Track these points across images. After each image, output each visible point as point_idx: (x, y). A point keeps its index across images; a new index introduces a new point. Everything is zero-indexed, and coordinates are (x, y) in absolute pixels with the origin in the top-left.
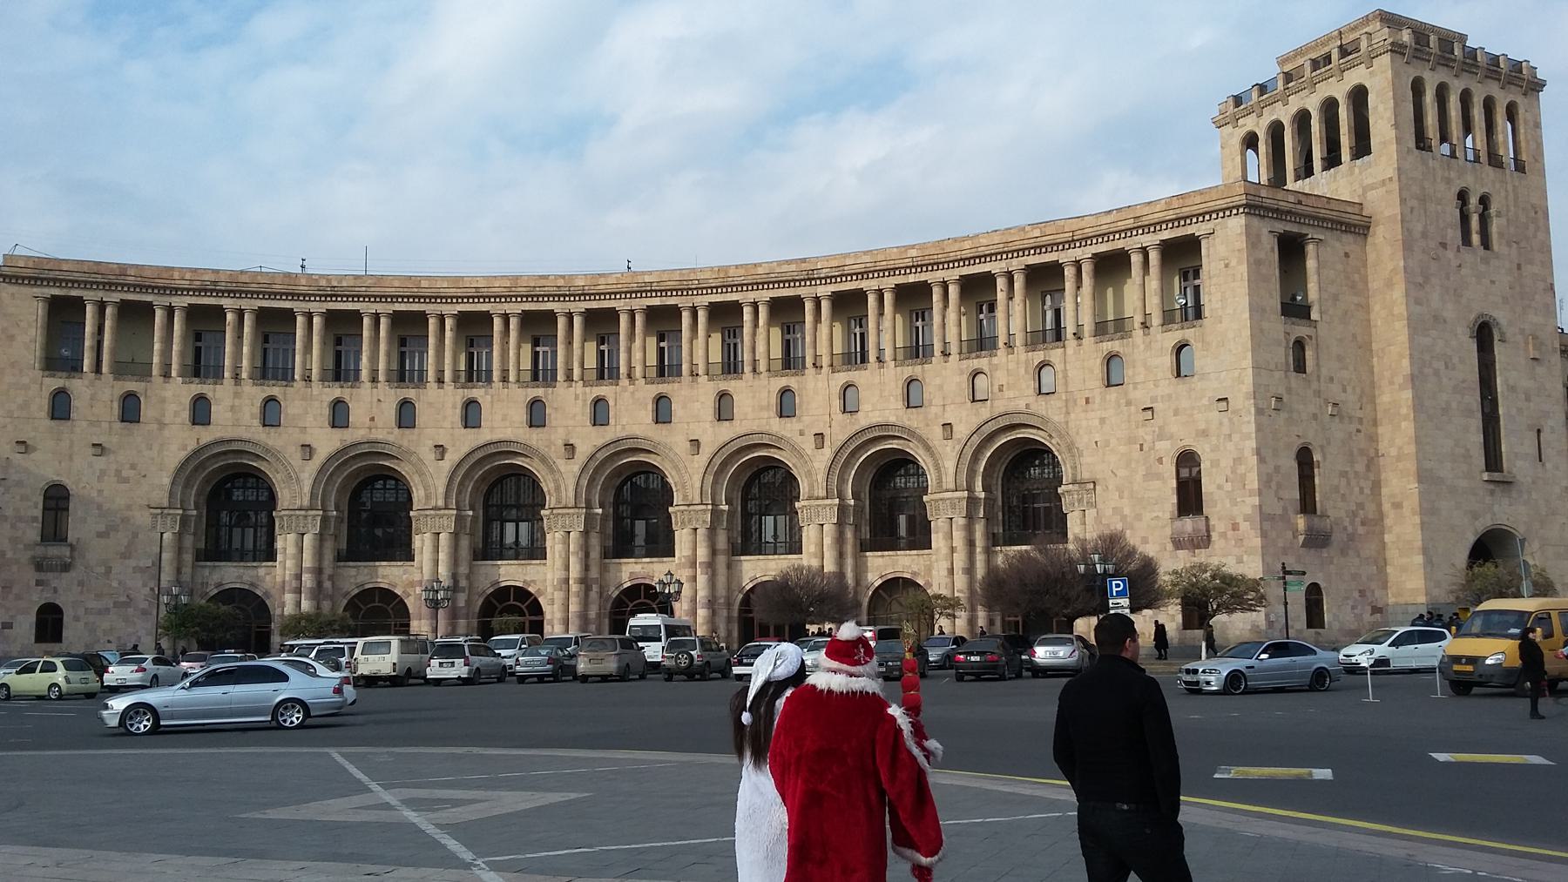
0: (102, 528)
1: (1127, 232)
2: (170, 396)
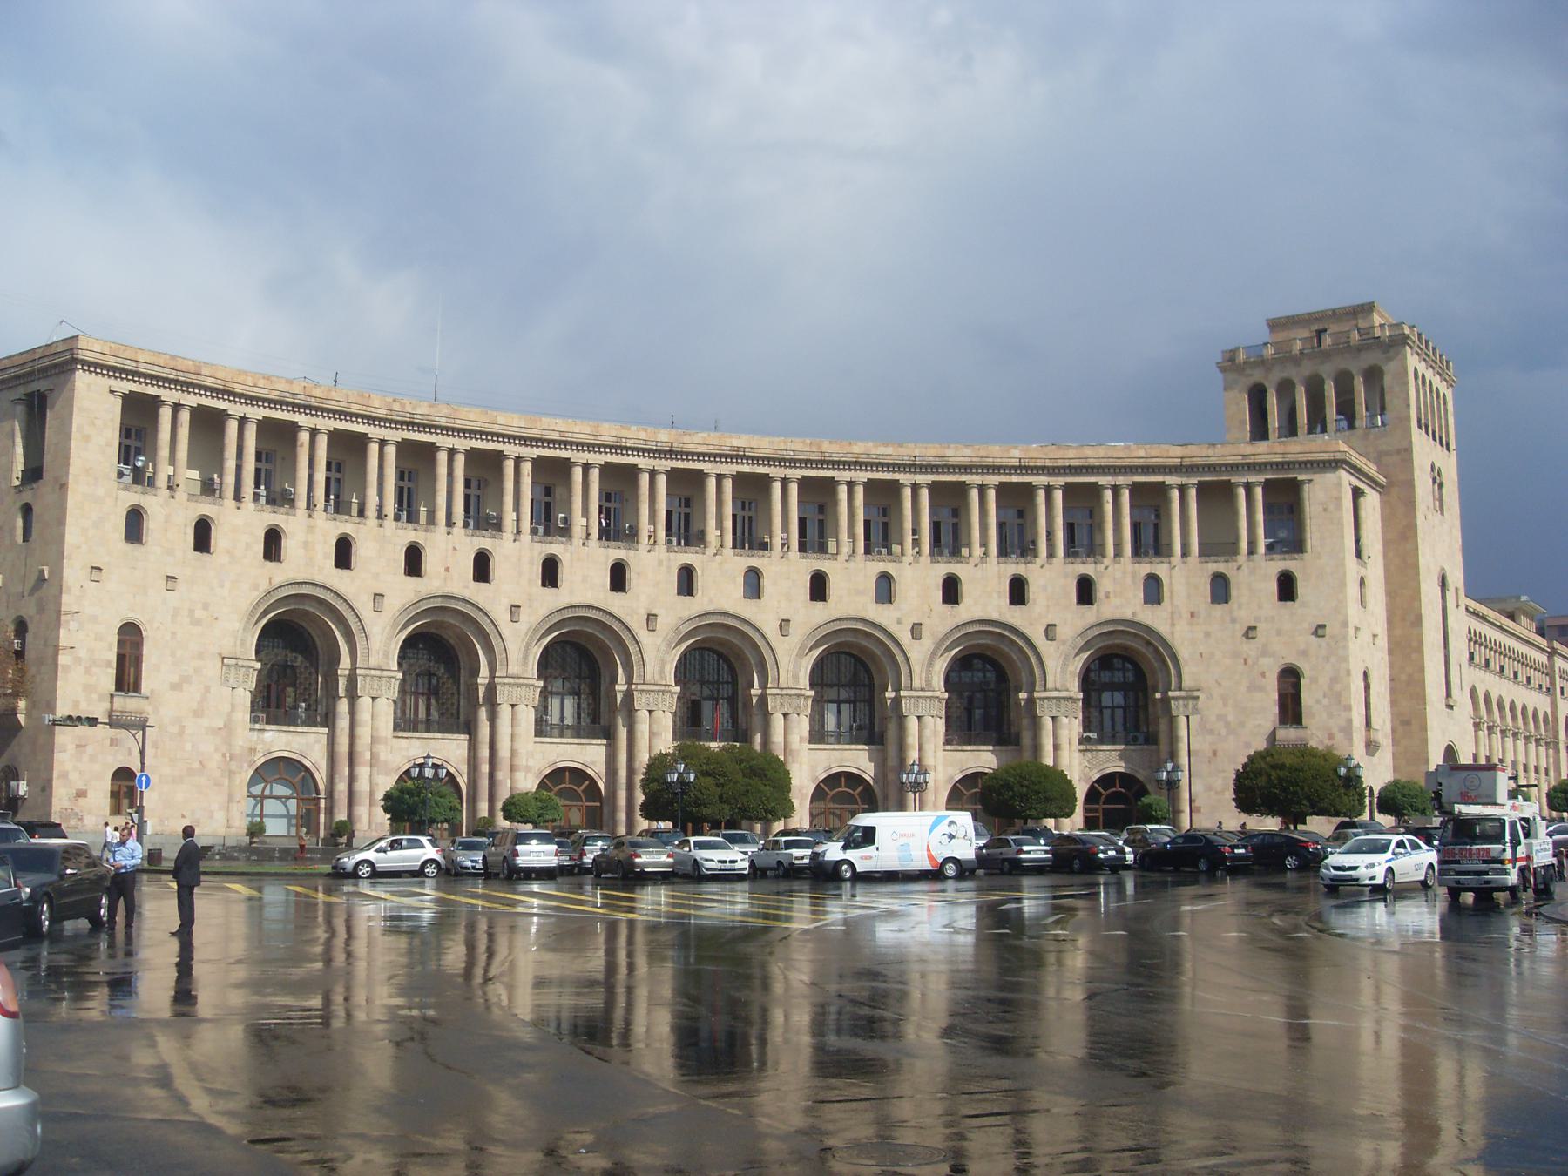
0: (175, 679)
1: (1234, 468)
2: (239, 525)
